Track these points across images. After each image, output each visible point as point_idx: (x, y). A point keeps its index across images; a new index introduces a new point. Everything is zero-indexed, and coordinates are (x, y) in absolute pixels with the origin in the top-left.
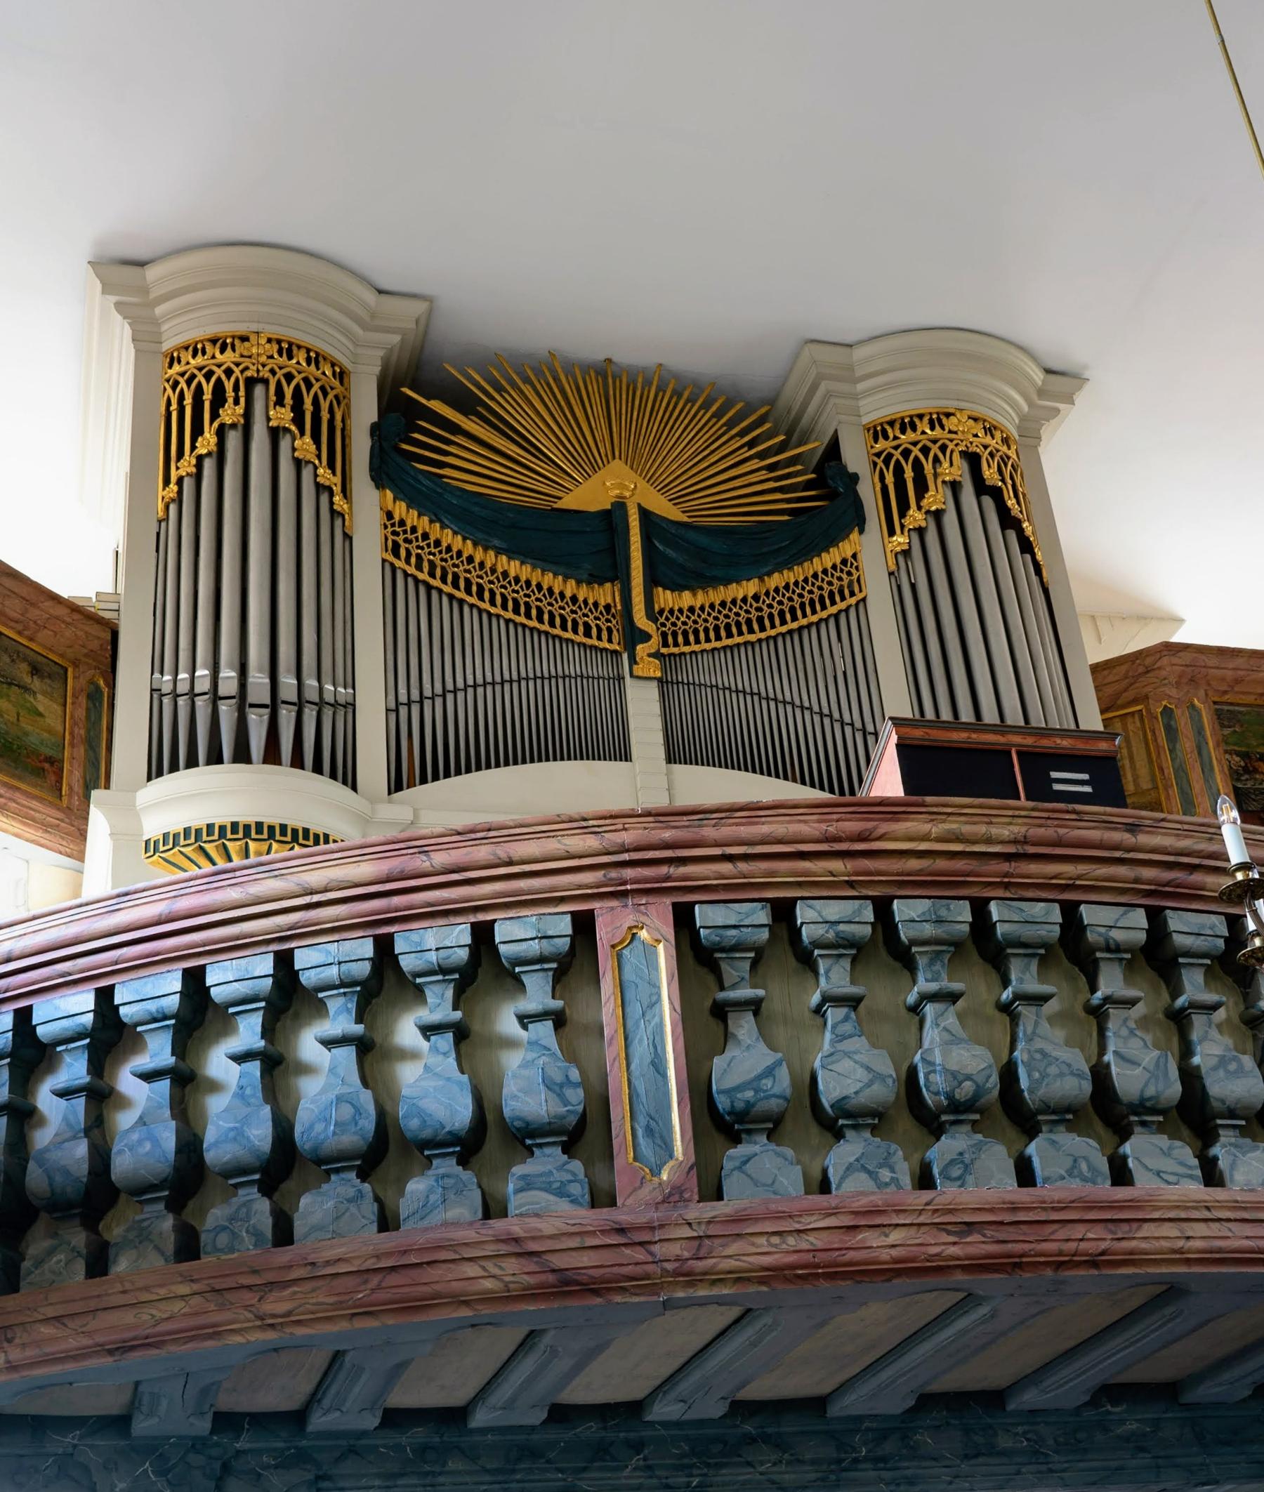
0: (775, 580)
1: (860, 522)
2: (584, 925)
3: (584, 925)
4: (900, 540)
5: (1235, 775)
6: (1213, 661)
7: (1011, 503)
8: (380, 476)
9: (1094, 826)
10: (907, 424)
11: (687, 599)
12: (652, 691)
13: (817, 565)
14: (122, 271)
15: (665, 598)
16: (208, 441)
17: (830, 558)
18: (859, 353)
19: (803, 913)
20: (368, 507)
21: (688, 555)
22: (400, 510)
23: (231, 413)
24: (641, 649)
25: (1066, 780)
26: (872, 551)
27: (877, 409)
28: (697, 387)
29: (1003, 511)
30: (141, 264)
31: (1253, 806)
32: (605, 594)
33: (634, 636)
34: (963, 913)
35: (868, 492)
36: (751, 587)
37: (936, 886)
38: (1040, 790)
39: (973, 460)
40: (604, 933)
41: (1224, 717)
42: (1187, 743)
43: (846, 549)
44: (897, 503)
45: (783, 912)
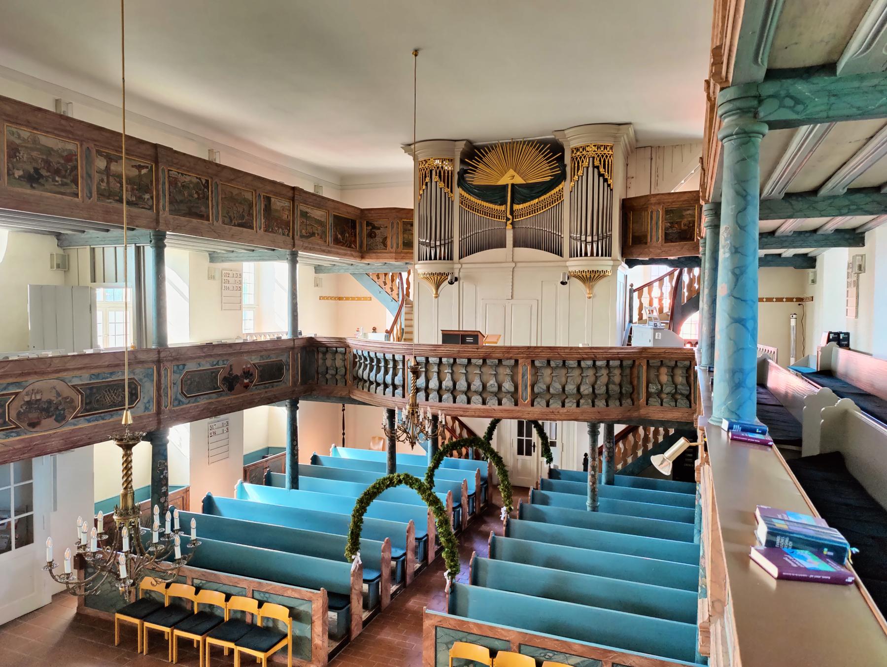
0: (542, 198)
1: (565, 178)
2: (404, 357)
3: (404, 357)
4: (573, 183)
5: (666, 229)
6: (667, 197)
7: (602, 170)
8: (459, 185)
9: (470, 348)
10: (578, 150)
11: (521, 206)
12: (512, 231)
13: (553, 192)
14: (408, 147)
15: (516, 207)
16: (424, 187)
17: (557, 189)
18: (566, 132)
19: (430, 359)
20: (458, 191)
21: (525, 193)
22: (463, 193)
23: (428, 179)
24: (508, 223)
25: (469, 340)
26: (566, 186)
27: (574, 144)
28: (533, 141)
29: (599, 172)
30: (410, 145)
31: (670, 237)
32: (503, 208)
33: (508, 219)
34: (452, 361)
35: (568, 169)
36: (536, 200)
37: (448, 357)
38: (463, 342)
39: (594, 158)
40: (406, 360)
41: (667, 212)
42: (654, 222)
43: (561, 186)
44: (574, 171)
45: (427, 359)
